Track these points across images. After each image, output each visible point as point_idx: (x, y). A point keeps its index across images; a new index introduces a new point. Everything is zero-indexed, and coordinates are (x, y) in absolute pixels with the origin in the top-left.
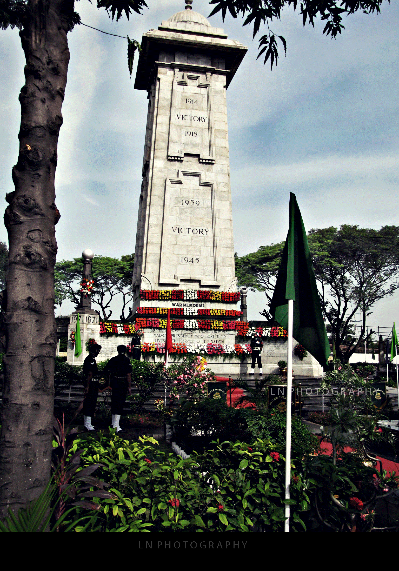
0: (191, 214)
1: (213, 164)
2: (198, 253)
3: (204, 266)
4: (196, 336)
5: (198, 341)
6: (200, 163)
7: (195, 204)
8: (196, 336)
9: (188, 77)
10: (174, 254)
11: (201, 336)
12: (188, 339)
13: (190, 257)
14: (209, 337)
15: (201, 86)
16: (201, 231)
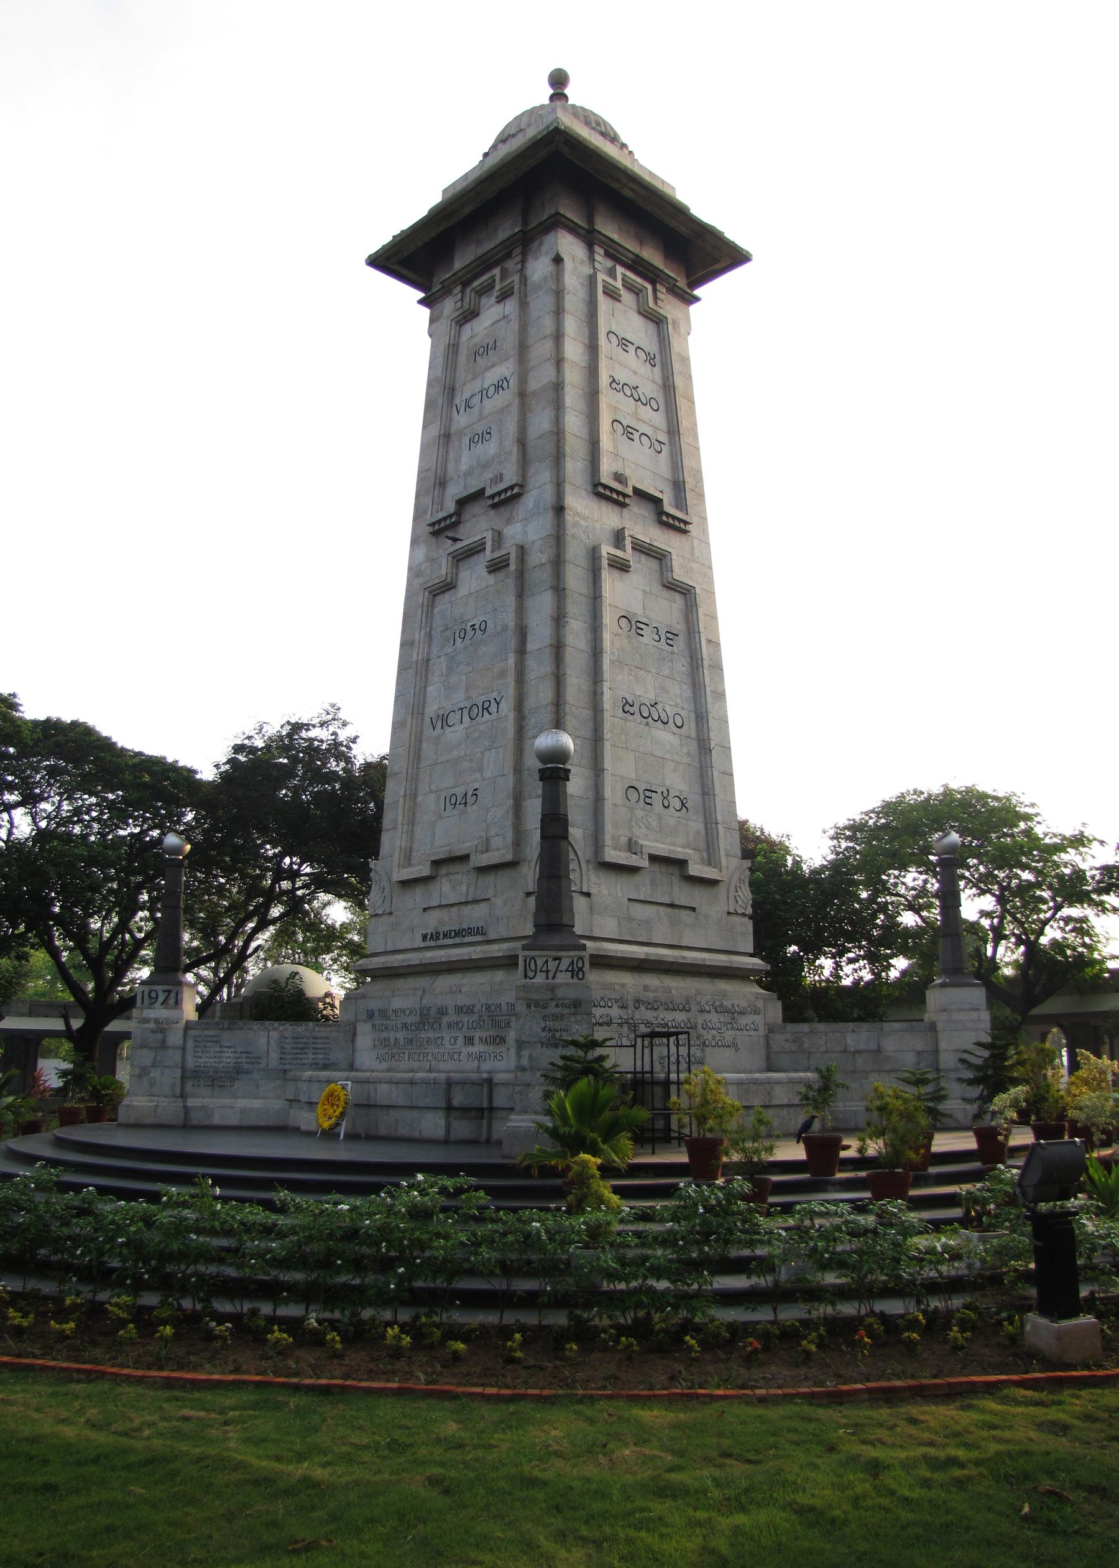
0: (468, 664)
1: (518, 496)
2: (478, 775)
3: (488, 810)
4: (449, 1026)
5: (452, 1040)
6: (494, 506)
7: (479, 632)
8: (449, 1026)
9: (477, 292)
10: (431, 792)
11: (457, 1023)
12: (431, 1035)
13: (459, 791)
14: (475, 1025)
15: (503, 297)
16: (486, 705)
